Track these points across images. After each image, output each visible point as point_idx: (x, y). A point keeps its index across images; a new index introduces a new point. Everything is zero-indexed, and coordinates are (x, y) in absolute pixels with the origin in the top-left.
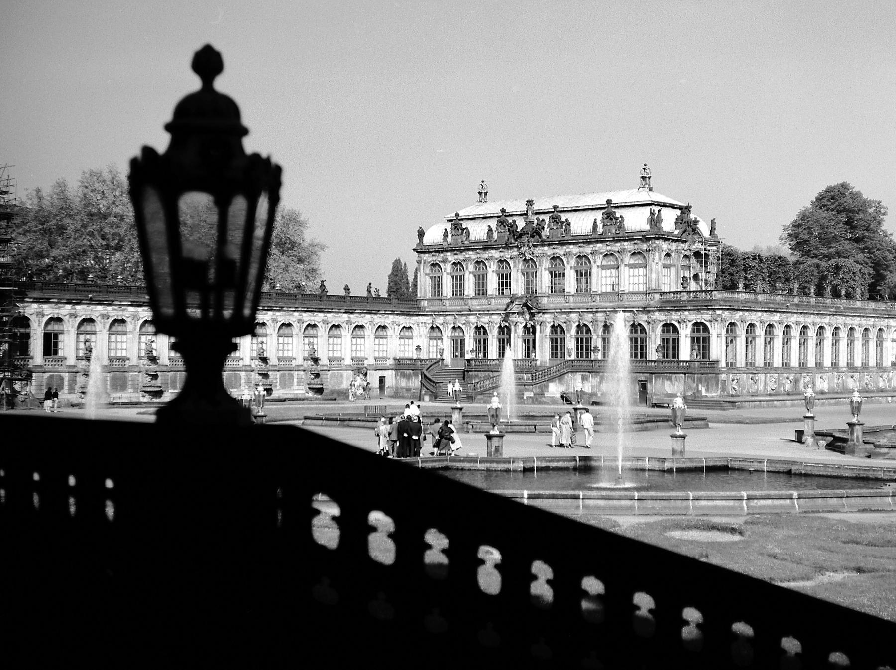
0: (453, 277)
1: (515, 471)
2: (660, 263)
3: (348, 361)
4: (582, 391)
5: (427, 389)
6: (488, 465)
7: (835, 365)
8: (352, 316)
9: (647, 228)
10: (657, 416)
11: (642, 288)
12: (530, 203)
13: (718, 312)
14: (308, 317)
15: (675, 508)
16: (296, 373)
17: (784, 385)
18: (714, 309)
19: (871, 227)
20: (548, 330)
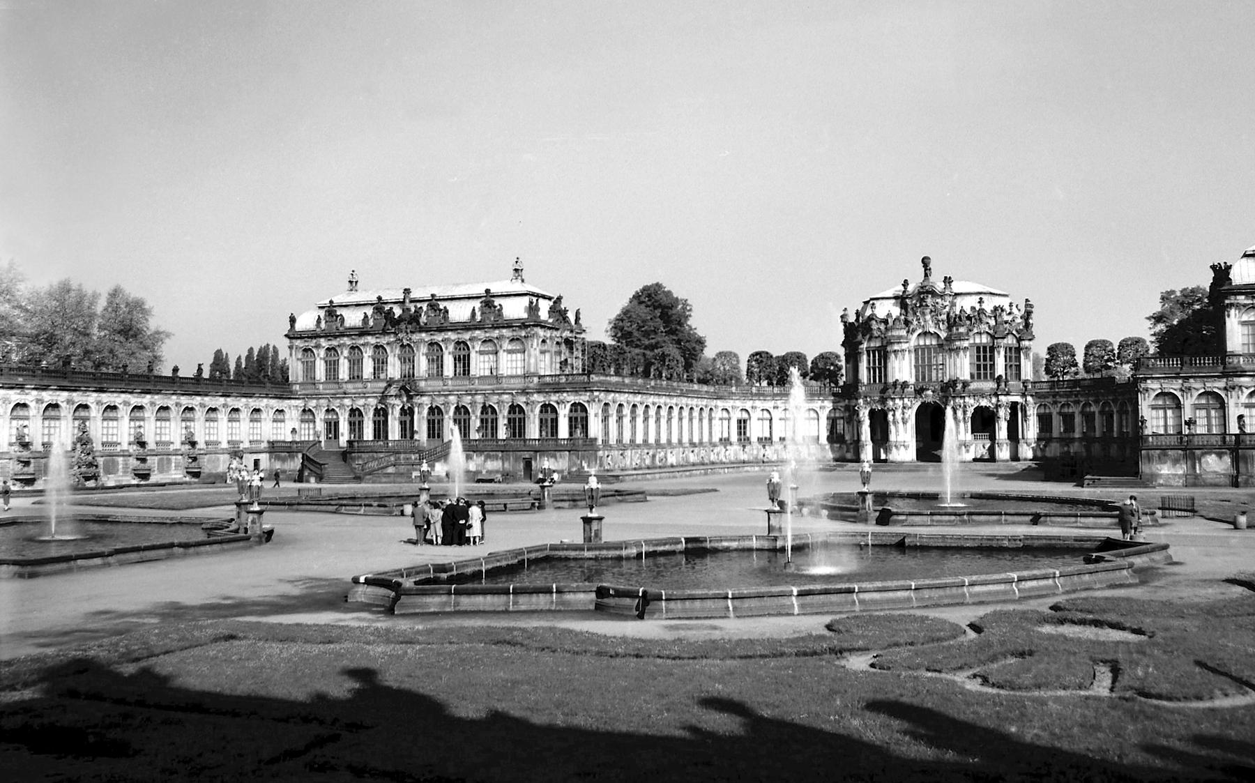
0: (326, 362)
1: (628, 558)
2: (538, 349)
3: (225, 445)
4: (549, 469)
5: (311, 470)
6: (597, 553)
7: (680, 442)
8: (228, 399)
9: (525, 316)
10: (607, 491)
11: (520, 372)
12: (407, 291)
13: (596, 394)
14: (185, 401)
15: (952, 597)
16: (174, 457)
18: (592, 391)
20: (426, 411)
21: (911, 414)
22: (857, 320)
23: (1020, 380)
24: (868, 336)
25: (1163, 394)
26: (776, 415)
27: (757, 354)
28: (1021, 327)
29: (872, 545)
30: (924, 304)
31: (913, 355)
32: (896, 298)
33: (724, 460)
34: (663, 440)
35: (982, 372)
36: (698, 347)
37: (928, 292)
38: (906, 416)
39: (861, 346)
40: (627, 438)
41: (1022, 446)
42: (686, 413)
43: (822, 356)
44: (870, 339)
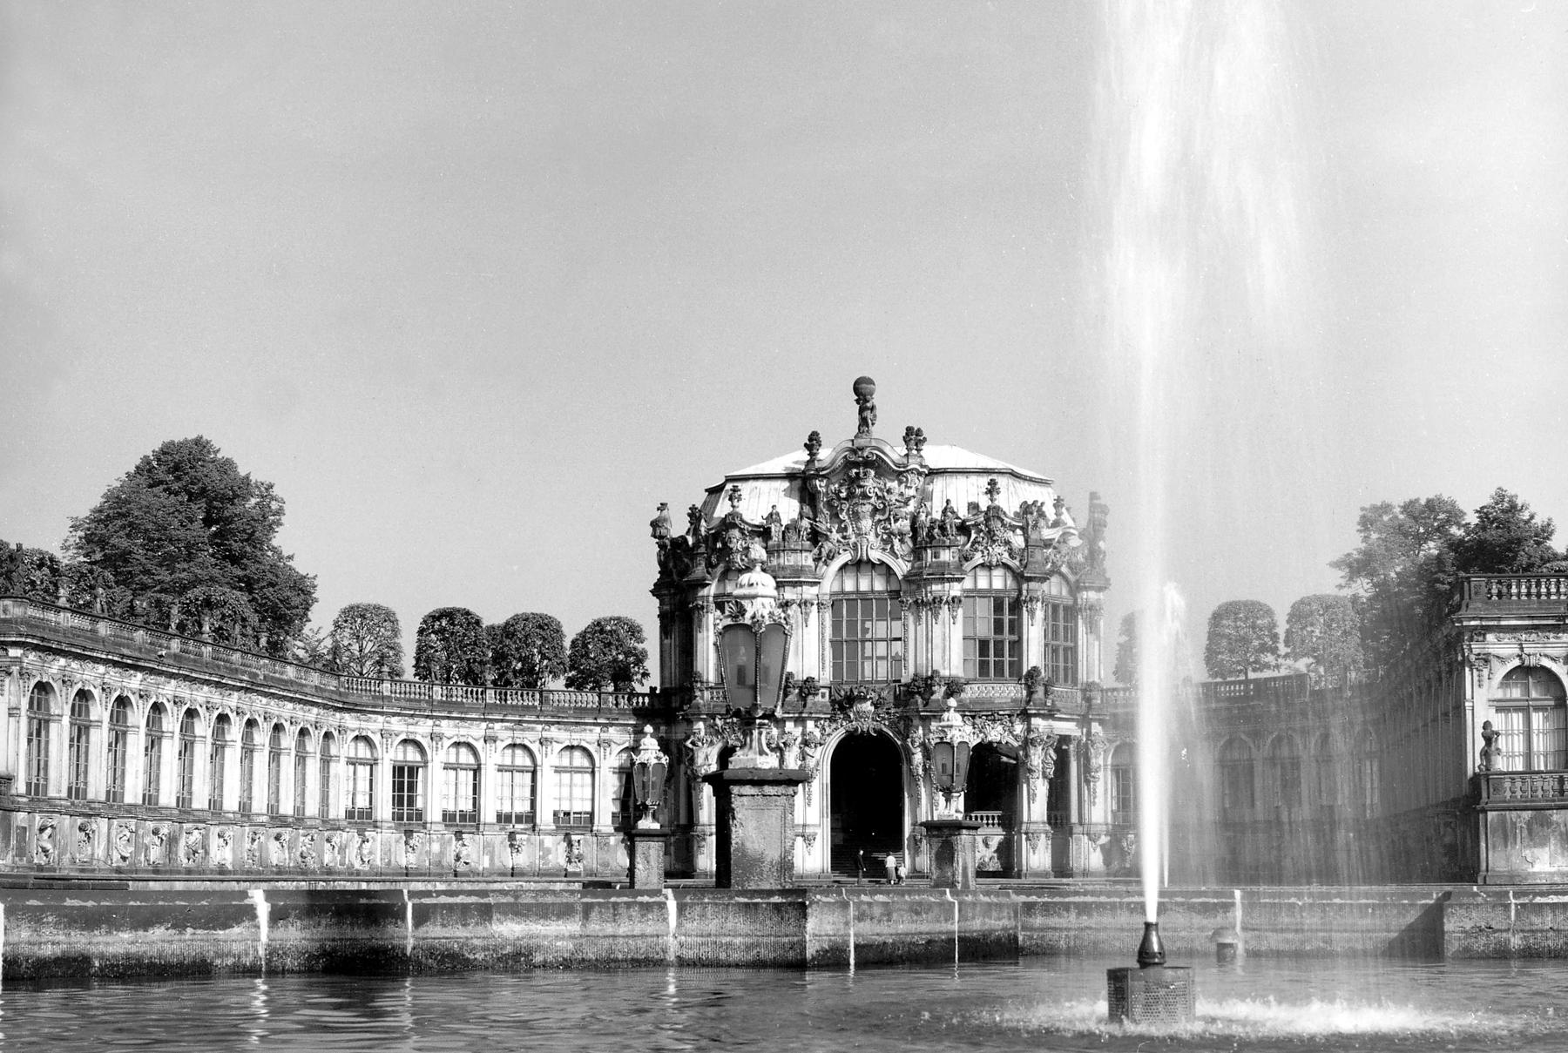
13: (14, 652)
17: (147, 848)
19: (257, 534)
21: (821, 759)
22: (695, 530)
23: (1075, 682)
24: (720, 569)
25: (1525, 672)
26: (492, 757)
27: (449, 614)
28: (1080, 558)
29: (1254, 954)
30: (858, 491)
31: (828, 616)
32: (790, 476)
33: (357, 865)
34: (200, 801)
35: (992, 659)
36: (296, 601)
37: (867, 464)
38: (811, 763)
39: (704, 592)
40: (97, 787)
41: (1080, 840)
42: (262, 737)
43: (598, 627)
44: (724, 577)
